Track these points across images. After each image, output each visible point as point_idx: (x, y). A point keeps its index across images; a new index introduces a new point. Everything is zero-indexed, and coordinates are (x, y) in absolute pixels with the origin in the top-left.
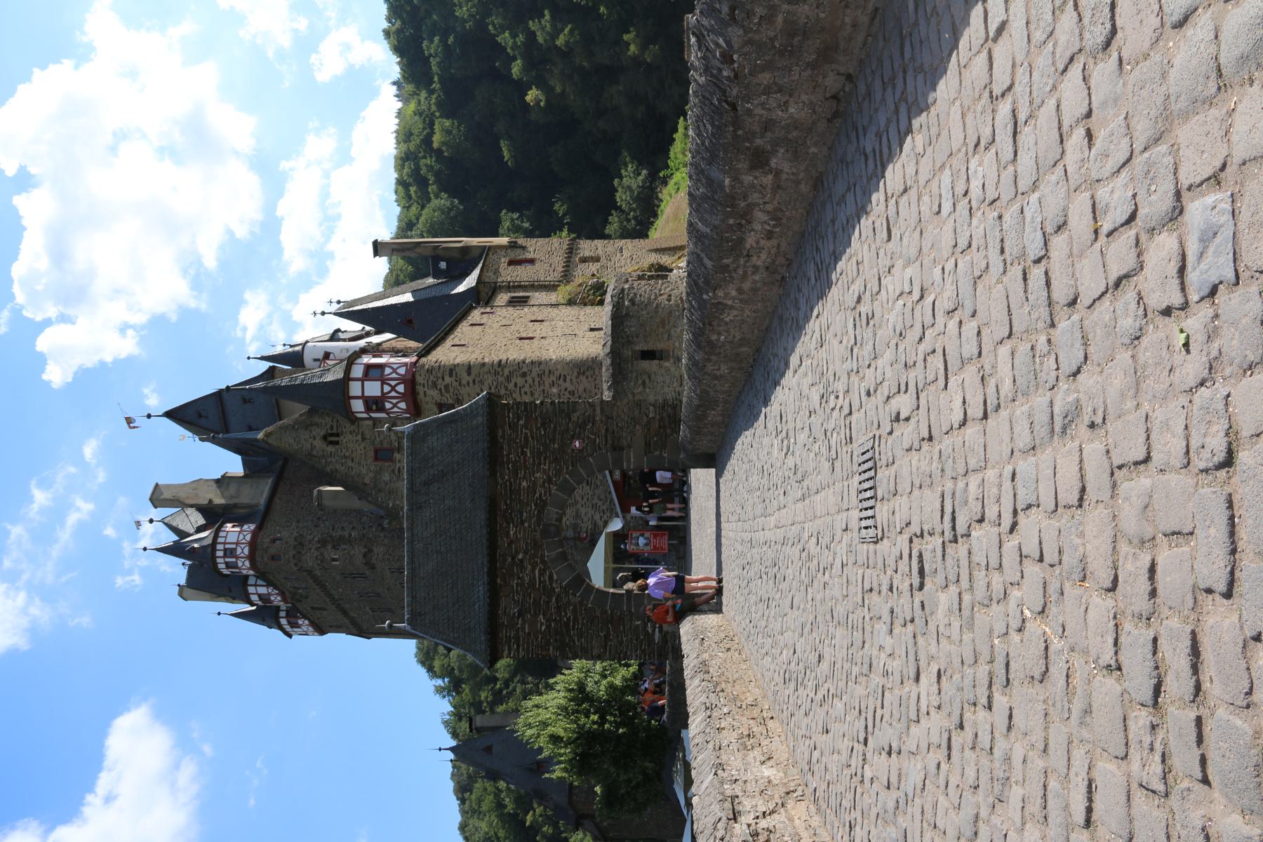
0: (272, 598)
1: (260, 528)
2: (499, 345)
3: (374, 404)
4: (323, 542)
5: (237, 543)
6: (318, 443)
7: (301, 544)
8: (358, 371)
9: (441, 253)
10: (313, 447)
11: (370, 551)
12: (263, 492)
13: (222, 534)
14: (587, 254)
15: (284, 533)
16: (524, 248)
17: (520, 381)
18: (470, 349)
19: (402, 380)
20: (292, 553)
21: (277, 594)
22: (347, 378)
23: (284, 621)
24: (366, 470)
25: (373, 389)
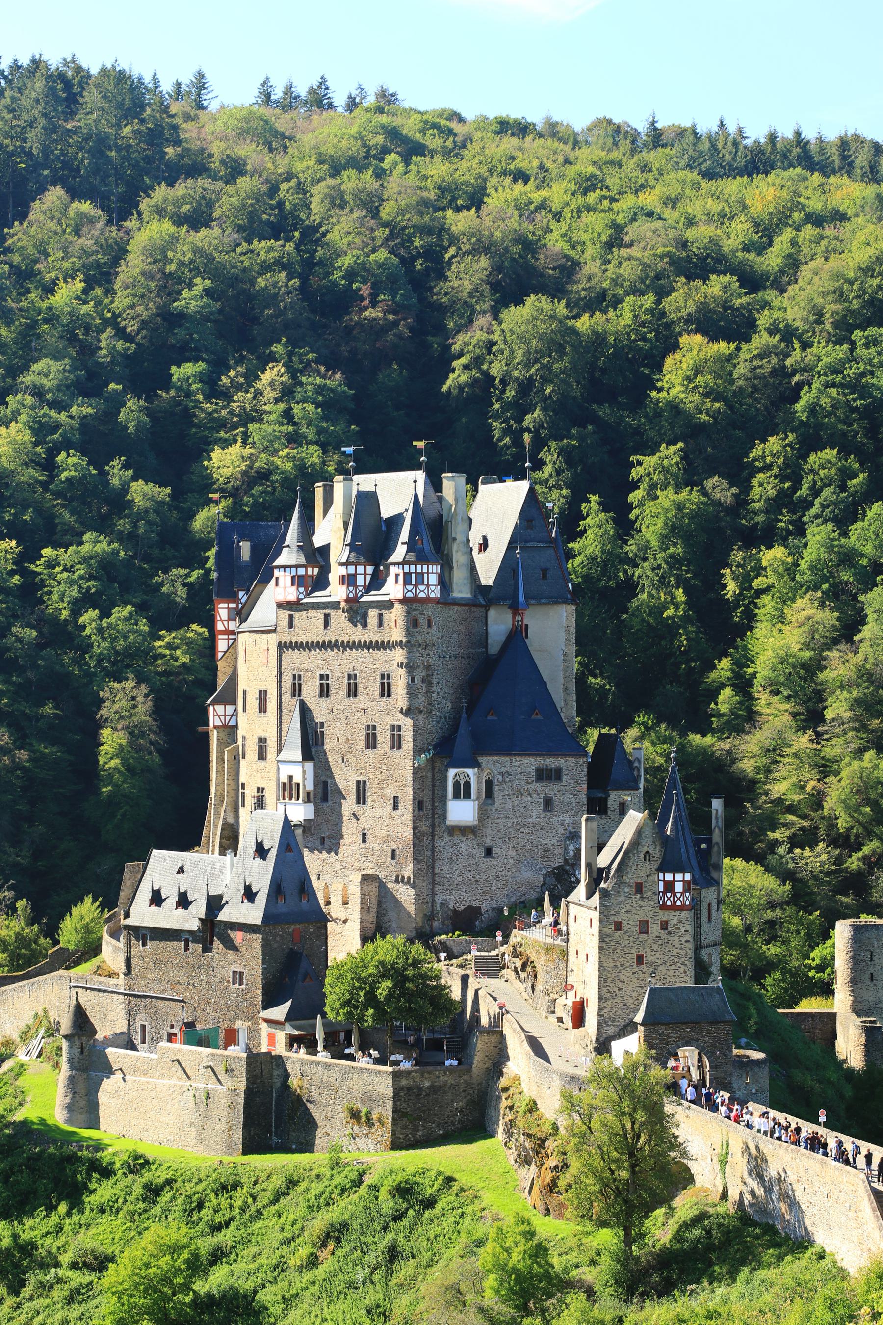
0: (351, 588)
1: (437, 601)
3: (669, 886)
4: (428, 668)
5: (428, 586)
6: (645, 849)
7: (427, 646)
9: (715, 849)
10: (643, 846)
11: (421, 712)
12: (460, 592)
17: (682, 970)
19: (683, 904)
20: (420, 639)
21: (356, 594)
23: (301, 571)
24: (631, 878)
25: (679, 887)
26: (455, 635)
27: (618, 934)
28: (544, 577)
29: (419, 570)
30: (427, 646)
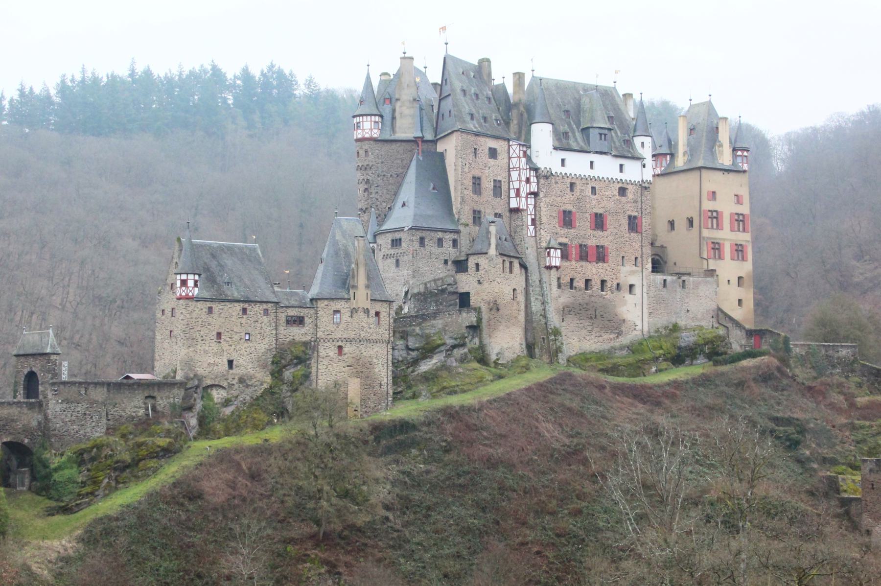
1: (376, 140)
2: (209, 327)
4: (368, 182)
5: (363, 129)
6: (175, 260)
7: (366, 169)
8: (184, 277)
11: (365, 212)
12: (406, 133)
13: (369, 117)
14: (345, 350)
15: (372, 157)
16: (352, 316)
18: (204, 316)
19: (181, 295)
22: (181, 274)
25: (178, 284)
26: (399, 161)
27: (164, 317)
28: (450, 116)
29: (358, 121)
30: (366, 169)
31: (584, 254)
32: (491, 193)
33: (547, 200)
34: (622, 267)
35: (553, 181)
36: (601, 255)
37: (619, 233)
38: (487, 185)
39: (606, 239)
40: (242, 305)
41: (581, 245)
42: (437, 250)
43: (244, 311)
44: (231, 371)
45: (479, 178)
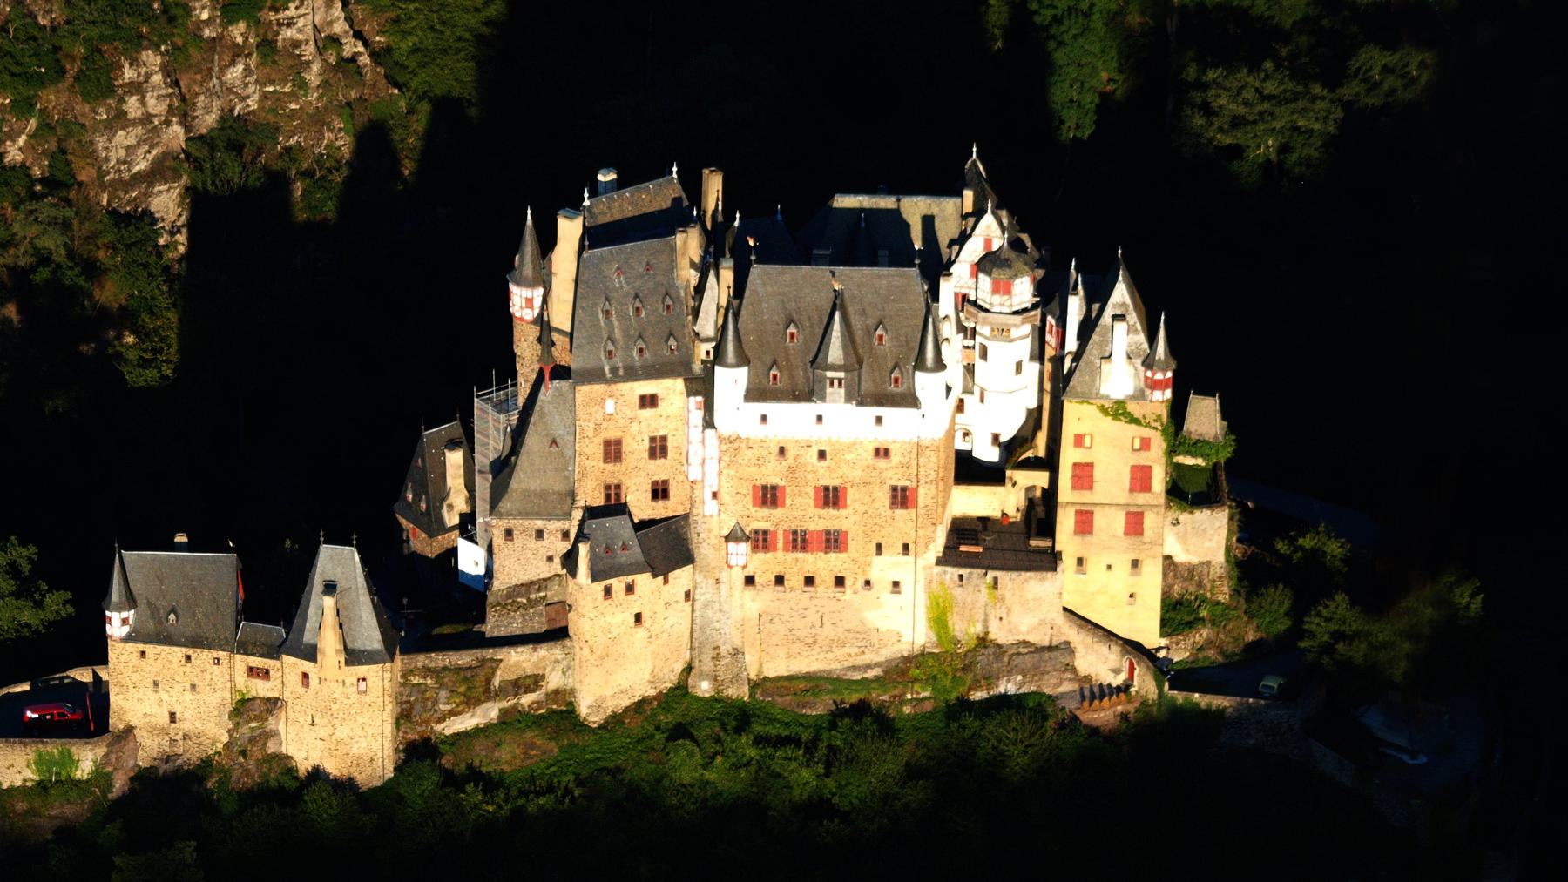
18: (135, 659)
31: (799, 541)
32: (646, 455)
33: (732, 472)
34: (877, 560)
35: (743, 445)
36: (834, 541)
37: (870, 511)
38: (635, 447)
39: (846, 521)
40: (184, 650)
41: (795, 532)
42: (534, 544)
43: (188, 658)
44: (173, 725)
45: (618, 442)
